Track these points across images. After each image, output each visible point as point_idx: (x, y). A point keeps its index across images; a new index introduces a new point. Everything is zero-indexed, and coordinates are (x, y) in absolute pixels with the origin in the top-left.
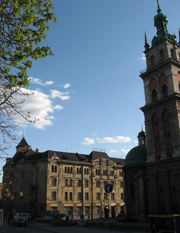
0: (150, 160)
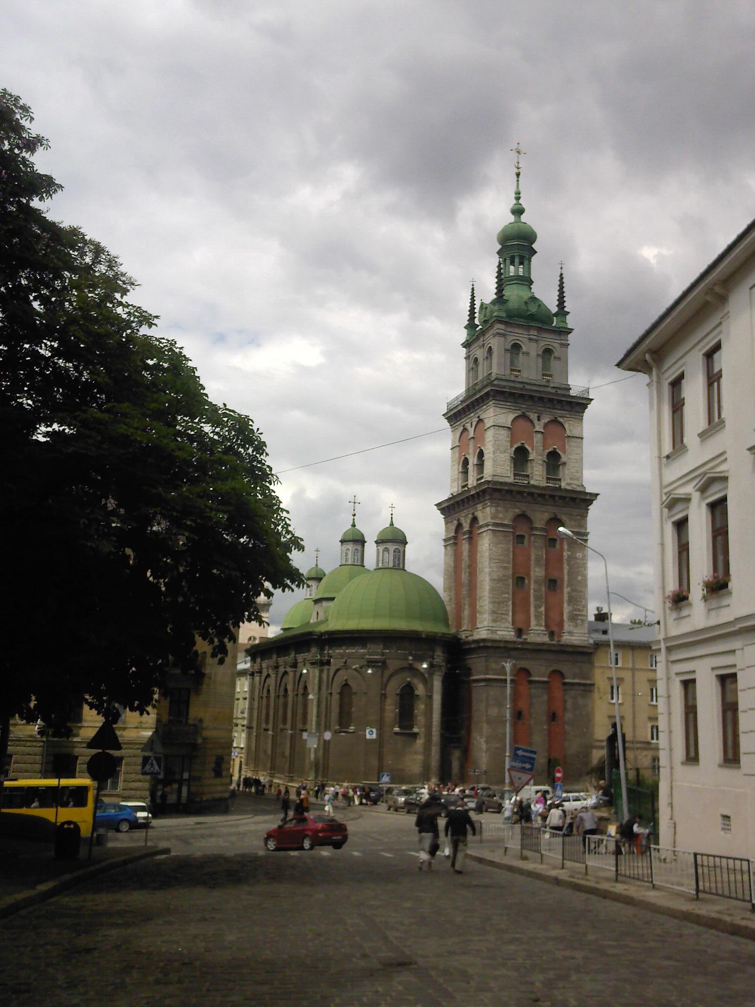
0: (499, 633)
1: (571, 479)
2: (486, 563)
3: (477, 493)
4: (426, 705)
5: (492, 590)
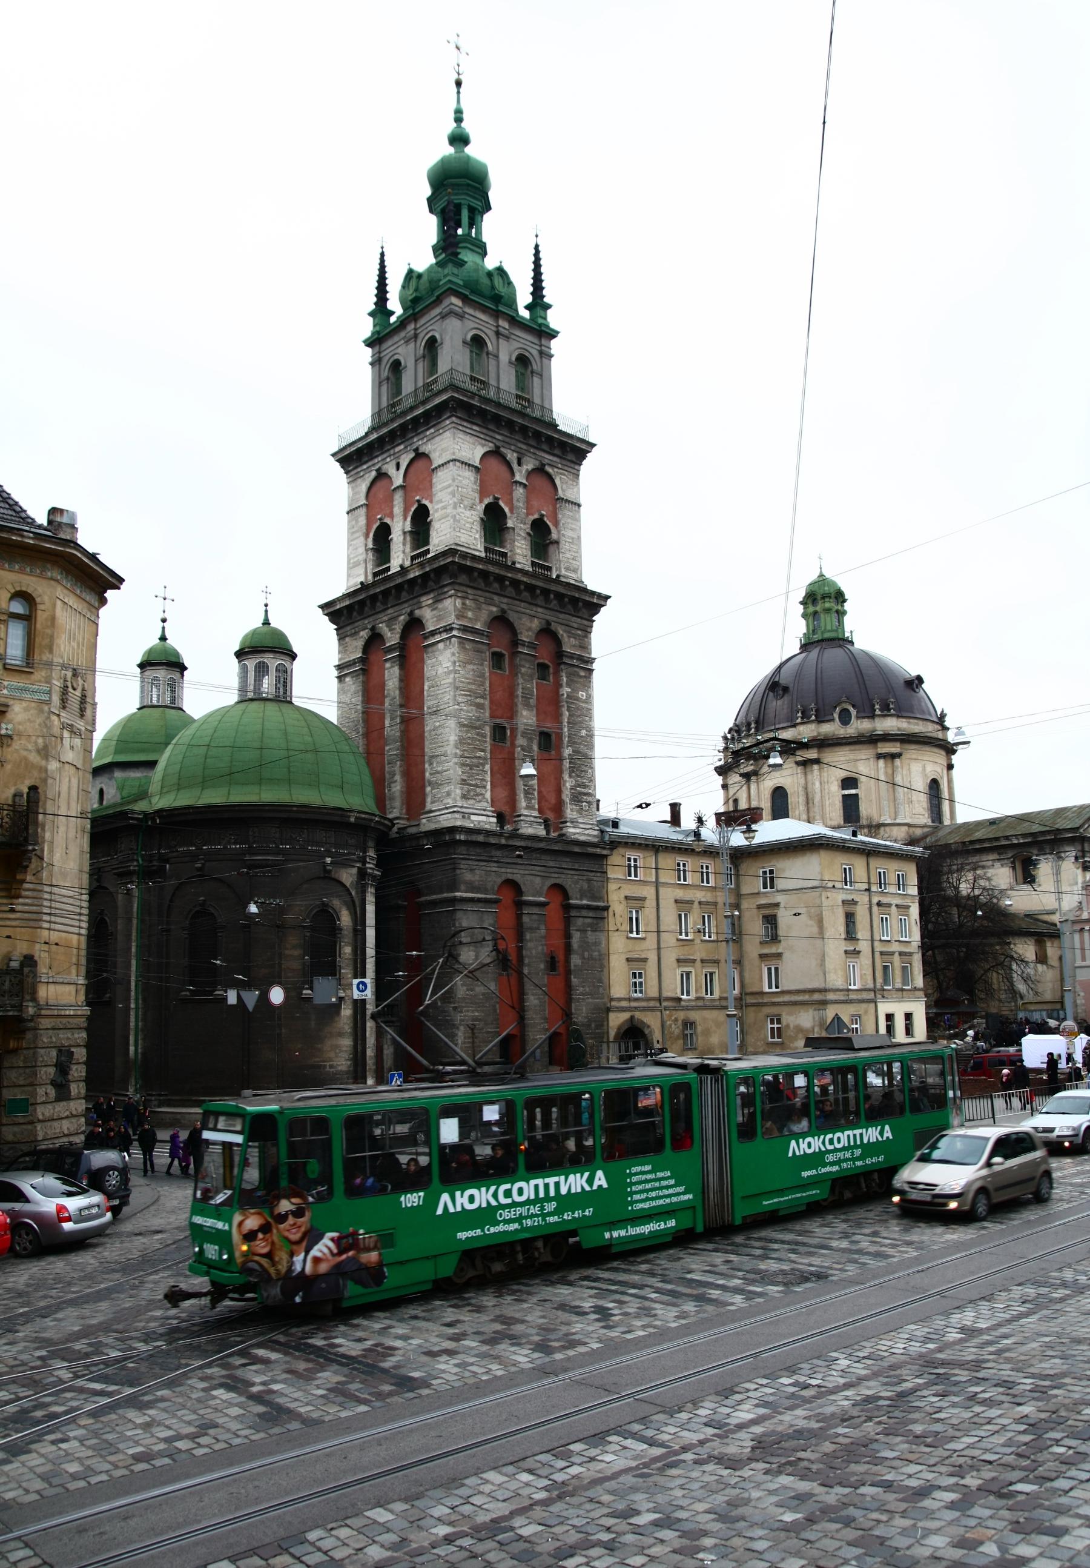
0: (473, 817)
1: (567, 569)
2: (448, 697)
3: (425, 577)
4: (355, 950)
5: (461, 741)
